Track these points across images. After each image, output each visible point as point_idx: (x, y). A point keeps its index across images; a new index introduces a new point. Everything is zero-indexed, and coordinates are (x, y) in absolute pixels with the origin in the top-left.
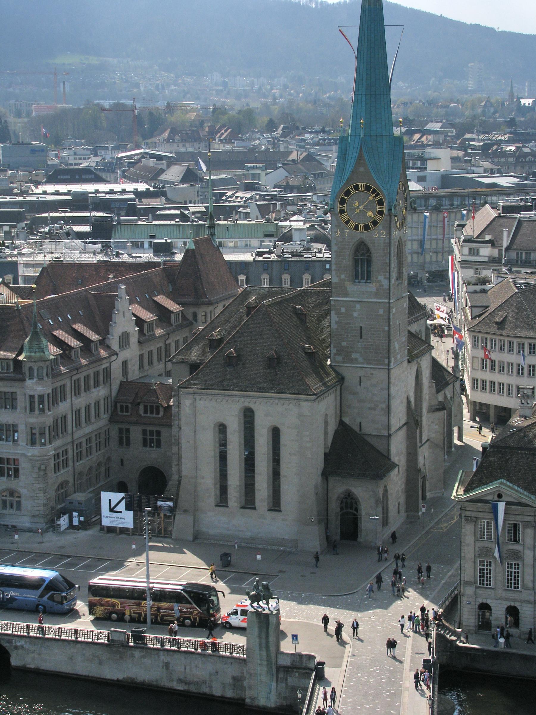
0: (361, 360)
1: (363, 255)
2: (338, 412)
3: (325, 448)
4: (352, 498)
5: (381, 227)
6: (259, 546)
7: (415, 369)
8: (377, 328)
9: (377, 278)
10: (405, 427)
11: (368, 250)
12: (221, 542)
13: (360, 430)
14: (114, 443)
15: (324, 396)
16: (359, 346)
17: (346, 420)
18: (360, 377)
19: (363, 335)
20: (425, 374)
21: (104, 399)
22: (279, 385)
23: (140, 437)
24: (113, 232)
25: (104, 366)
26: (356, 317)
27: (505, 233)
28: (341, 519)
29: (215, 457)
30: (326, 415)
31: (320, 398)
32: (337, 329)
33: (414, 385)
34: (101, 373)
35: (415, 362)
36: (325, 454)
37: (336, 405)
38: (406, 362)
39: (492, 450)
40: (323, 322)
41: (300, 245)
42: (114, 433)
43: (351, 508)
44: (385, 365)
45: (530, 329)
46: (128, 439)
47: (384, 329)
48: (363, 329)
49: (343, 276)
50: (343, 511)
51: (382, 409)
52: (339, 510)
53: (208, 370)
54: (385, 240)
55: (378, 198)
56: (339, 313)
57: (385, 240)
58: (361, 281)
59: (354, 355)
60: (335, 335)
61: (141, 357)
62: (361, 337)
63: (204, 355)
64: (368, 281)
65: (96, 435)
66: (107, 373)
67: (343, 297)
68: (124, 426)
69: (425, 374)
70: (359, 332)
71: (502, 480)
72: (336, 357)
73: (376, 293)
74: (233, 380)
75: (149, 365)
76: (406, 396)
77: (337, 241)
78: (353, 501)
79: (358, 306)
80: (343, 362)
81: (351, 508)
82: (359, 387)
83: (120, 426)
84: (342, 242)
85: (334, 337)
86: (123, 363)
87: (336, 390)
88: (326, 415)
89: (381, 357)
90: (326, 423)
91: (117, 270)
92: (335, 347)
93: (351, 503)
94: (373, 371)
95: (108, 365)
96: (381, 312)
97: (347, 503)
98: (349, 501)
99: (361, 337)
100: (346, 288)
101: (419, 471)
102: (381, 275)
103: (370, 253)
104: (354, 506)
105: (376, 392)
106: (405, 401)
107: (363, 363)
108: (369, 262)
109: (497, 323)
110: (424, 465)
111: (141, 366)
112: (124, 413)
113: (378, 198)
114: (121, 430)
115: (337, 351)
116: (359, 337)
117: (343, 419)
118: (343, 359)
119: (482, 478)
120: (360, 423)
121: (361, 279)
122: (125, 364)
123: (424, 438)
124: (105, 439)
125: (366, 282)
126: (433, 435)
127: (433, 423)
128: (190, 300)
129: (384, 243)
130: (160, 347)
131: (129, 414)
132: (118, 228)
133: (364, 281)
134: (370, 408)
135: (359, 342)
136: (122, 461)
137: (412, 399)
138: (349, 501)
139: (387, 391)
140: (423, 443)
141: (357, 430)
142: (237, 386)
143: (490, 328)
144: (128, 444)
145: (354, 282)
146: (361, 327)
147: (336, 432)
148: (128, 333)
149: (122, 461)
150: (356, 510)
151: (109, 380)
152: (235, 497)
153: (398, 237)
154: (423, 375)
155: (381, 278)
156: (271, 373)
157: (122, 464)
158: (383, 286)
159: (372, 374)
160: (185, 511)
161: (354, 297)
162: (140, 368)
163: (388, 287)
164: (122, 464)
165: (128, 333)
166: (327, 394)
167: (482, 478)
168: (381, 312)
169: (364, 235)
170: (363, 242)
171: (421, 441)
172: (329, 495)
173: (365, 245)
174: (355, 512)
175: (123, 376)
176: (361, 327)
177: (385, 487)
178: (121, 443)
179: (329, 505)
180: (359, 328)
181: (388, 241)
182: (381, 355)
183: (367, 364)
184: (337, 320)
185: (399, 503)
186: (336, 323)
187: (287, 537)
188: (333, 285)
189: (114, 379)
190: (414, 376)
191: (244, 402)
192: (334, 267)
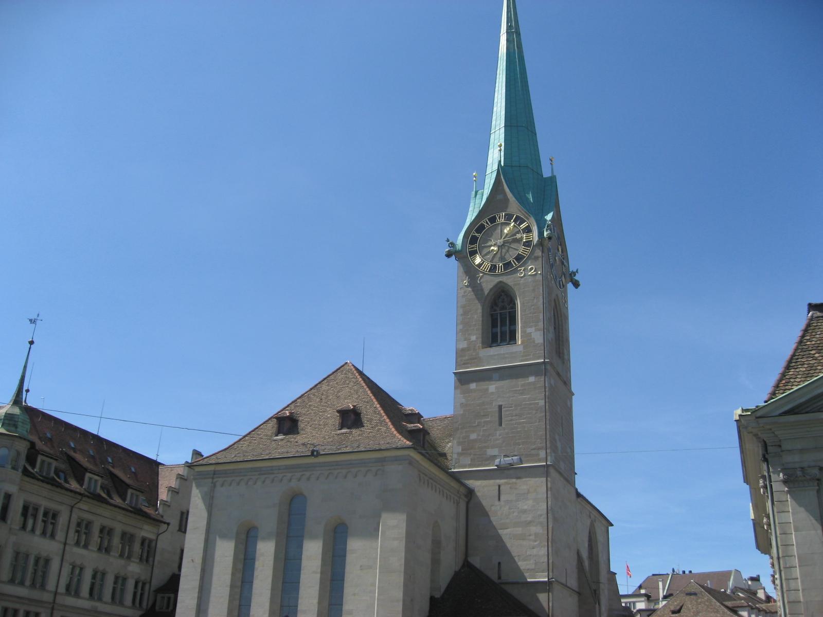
1: (503, 308)
13: (499, 578)
17: (476, 561)
18: (499, 486)
26: (492, 393)
27: (660, 584)
36: (432, 599)
44: (540, 461)
45: (715, 612)
49: (473, 338)
51: (536, 535)
58: (501, 344)
59: (491, 452)
62: (500, 424)
64: (511, 343)
70: (497, 415)
80: (470, 466)
82: (497, 503)
90: (437, 544)
102: (531, 327)
105: (526, 507)
115: (462, 450)
116: (497, 423)
117: (471, 560)
120: (499, 563)
121: (501, 343)
133: (505, 344)
137: (586, 563)
139: (546, 503)
141: (494, 577)
170: (503, 291)
176: (500, 407)
180: (497, 409)
191: (290, 480)
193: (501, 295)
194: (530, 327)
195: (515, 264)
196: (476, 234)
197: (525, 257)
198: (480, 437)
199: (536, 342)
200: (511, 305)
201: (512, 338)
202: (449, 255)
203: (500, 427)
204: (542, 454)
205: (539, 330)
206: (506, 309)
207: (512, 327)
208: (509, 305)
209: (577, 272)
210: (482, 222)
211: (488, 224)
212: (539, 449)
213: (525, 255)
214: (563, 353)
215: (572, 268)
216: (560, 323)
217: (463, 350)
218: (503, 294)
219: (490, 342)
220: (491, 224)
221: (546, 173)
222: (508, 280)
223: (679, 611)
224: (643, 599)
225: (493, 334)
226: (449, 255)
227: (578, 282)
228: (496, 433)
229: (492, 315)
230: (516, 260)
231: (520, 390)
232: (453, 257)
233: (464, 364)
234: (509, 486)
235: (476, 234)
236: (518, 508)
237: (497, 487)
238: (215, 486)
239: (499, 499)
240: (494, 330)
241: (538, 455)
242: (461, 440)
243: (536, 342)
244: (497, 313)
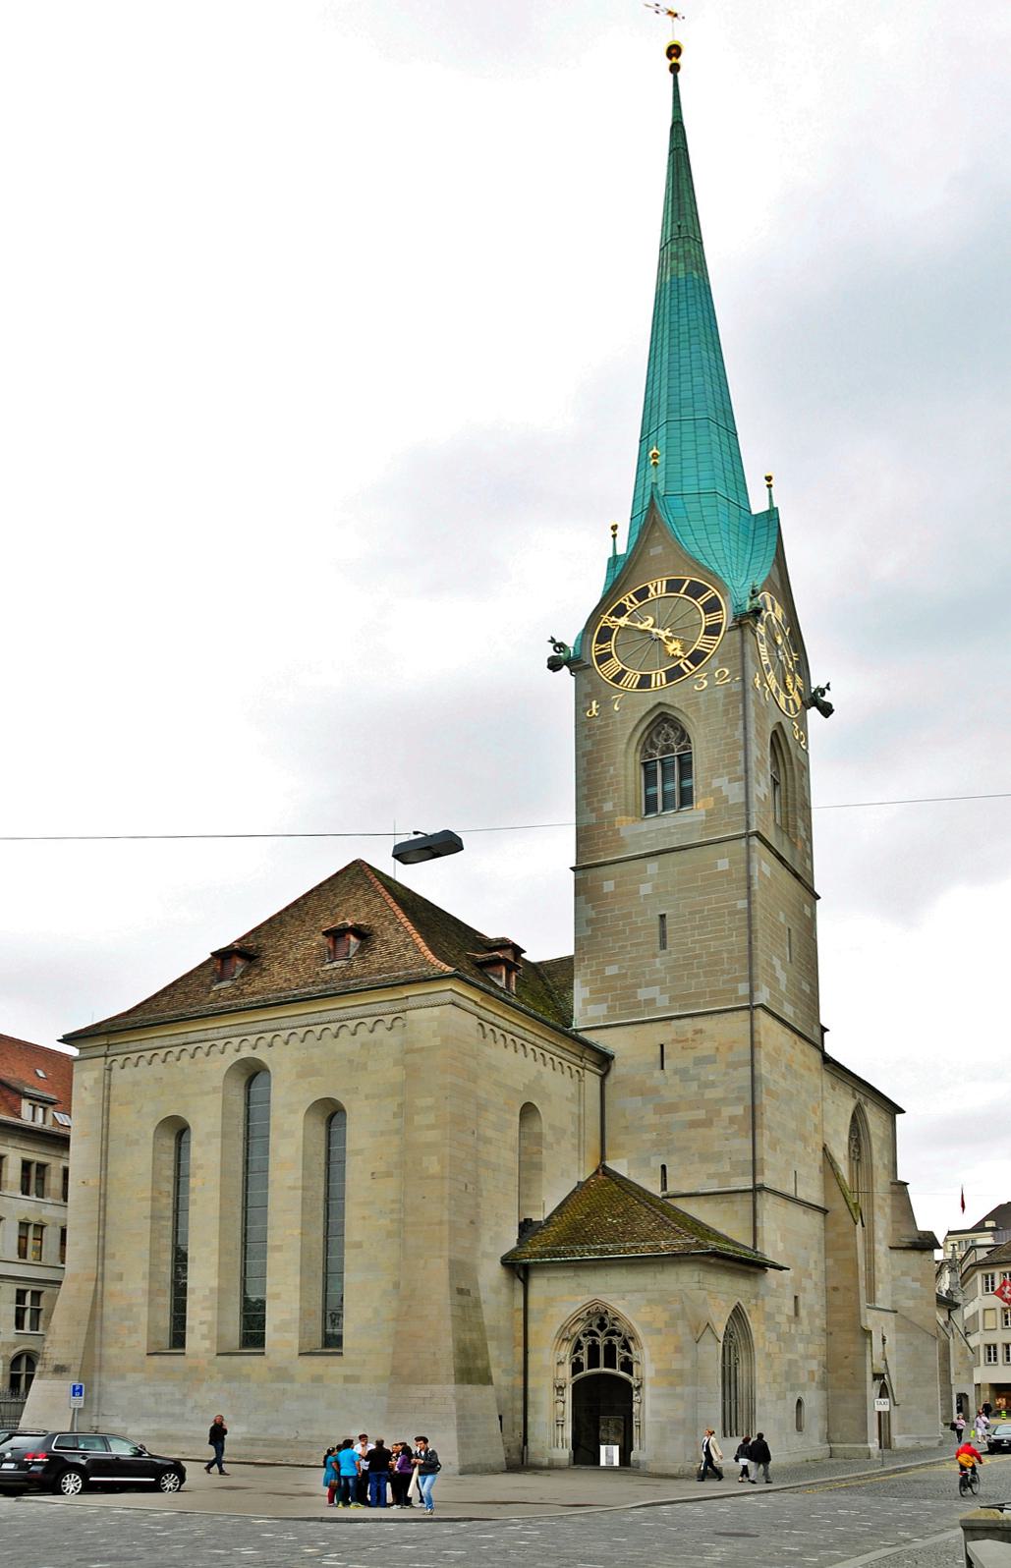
4: (612, 1333)
5: (715, 662)
8: (708, 910)
11: (684, 735)
16: (658, 966)
44: (737, 999)
70: (657, 930)
78: (616, 1340)
79: (652, 867)
81: (610, 1363)
89: (725, 982)
93: (610, 1349)
94: (700, 1023)
97: (593, 1349)
98: (602, 1341)
99: (663, 946)
104: (620, 1354)
134: (694, 1124)
138: (602, 1341)
145: (643, 819)
150: (627, 1366)
163: (742, 799)
173: (675, 724)
174: (623, 1374)
180: (657, 922)
181: (737, 688)
182: (726, 977)
193: (663, 729)
194: (718, 777)
197: (708, 654)
200: (682, 744)
201: (686, 797)
202: (554, 665)
203: (664, 951)
207: (686, 783)
208: (679, 744)
209: (829, 689)
210: (621, 601)
211: (631, 602)
212: (737, 980)
213: (708, 651)
215: (816, 682)
219: (644, 813)
220: (640, 602)
221: (758, 505)
222: (671, 695)
225: (647, 797)
226: (554, 665)
227: (831, 705)
228: (655, 962)
229: (645, 765)
230: (690, 661)
231: (698, 887)
232: (565, 669)
234: (680, 1045)
236: (699, 1080)
237: (659, 1048)
238: (110, 1070)
240: (651, 791)
241: (735, 990)
244: (656, 761)
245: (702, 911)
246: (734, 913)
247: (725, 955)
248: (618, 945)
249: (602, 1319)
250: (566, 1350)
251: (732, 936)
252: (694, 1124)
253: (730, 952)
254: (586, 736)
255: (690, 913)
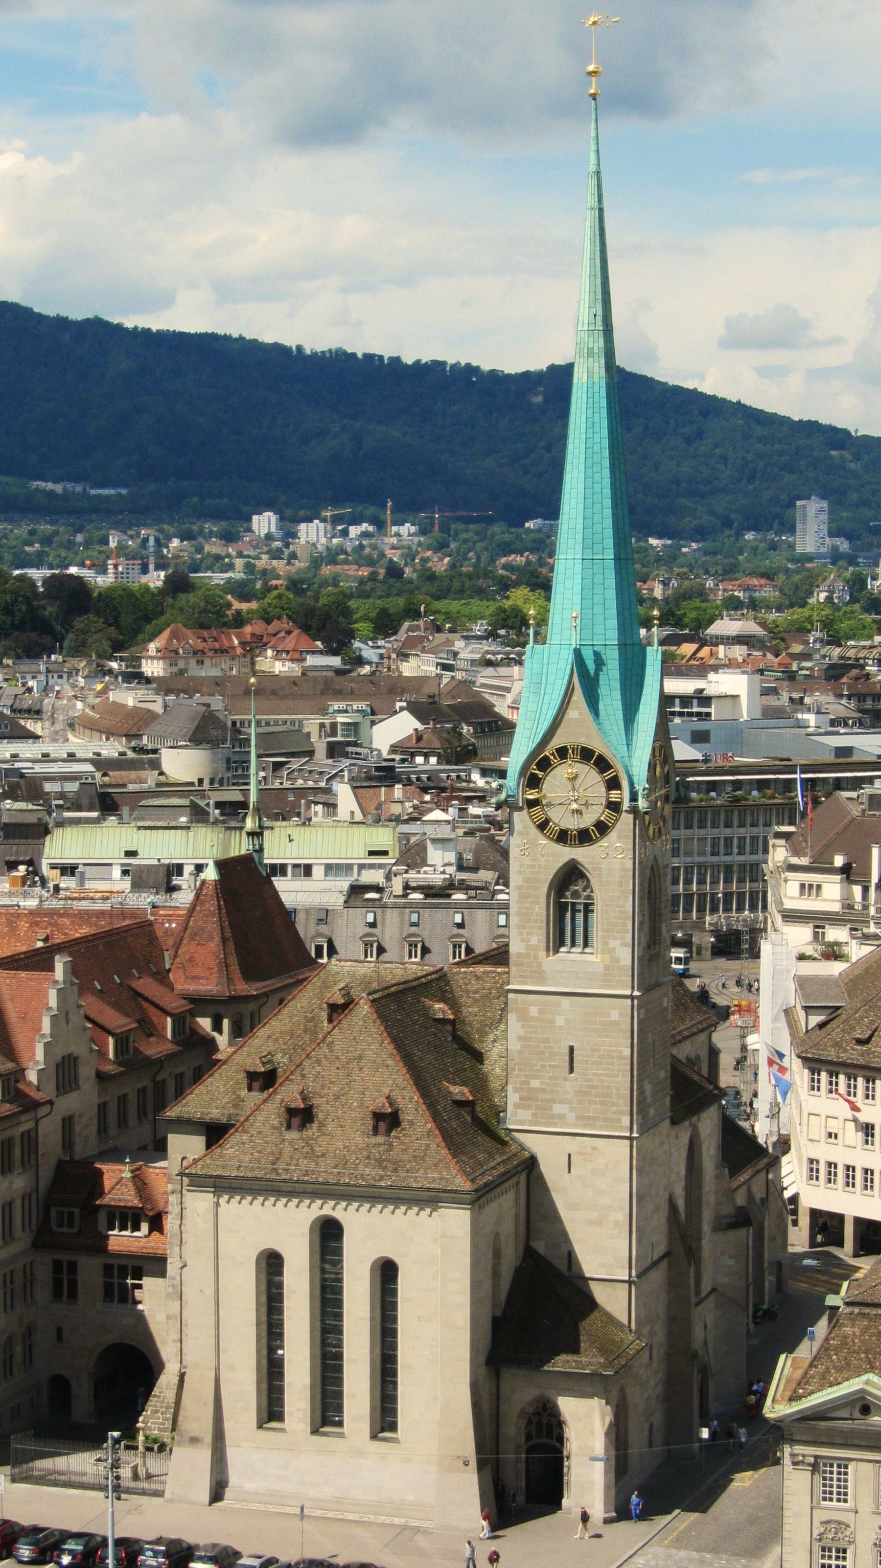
0: (571, 1117)
1: (576, 895)
2: (522, 1229)
3: (494, 1306)
6: (351, 1517)
7: (685, 1139)
9: (605, 944)
10: (664, 1264)
12: (270, 1508)
14: (43, 1294)
15: (492, 1195)
17: (540, 1246)
18: (570, 1155)
19: (575, 1065)
20: (708, 1149)
21: (23, 1198)
22: (395, 1170)
23: (99, 1280)
24: (47, 843)
25: (23, 1128)
26: (560, 1027)
28: (527, 1459)
29: (258, 1324)
30: (497, 1235)
31: (484, 1200)
32: (520, 1052)
33: (683, 1172)
34: (18, 1142)
35: (687, 1123)
37: (517, 1217)
38: (667, 1122)
39: (849, 1310)
40: (491, 1037)
41: (443, 872)
42: (44, 1273)
43: (550, 1434)
44: (622, 1129)
46: (73, 1284)
47: (621, 1051)
48: (575, 1052)
50: (531, 1443)
51: (616, 1223)
52: (523, 1437)
53: (245, 1137)
54: (623, 864)
55: (609, 775)
56: (524, 1018)
57: (623, 864)
58: (573, 950)
59: (558, 1109)
60: (516, 1064)
61: (102, 1108)
62: (571, 1070)
63: (236, 1106)
64: (587, 950)
65: (5, 1275)
66: (30, 1141)
67: (532, 984)
68: (65, 1257)
69: (708, 1149)
70: (567, 1058)
71: (870, 1376)
72: (519, 1111)
73: (605, 975)
74: (298, 1160)
75: (119, 1126)
76: (667, 1197)
77: (521, 865)
78: (554, 1421)
80: (531, 1123)
82: (566, 1175)
83: (57, 1256)
84: (533, 866)
85: (514, 1069)
86: (63, 1120)
87: (518, 1183)
88: (497, 1235)
89: (614, 1112)
90: (497, 1253)
91: (56, 924)
92: (516, 1090)
93: (549, 1425)
95: (29, 1126)
96: (615, 1016)
97: (539, 1423)
99: (571, 1070)
100: (540, 965)
101: (695, 1355)
103: (592, 891)
106: (665, 1206)
107: (574, 1126)
108: (588, 909)
109: (859, 1042)
110: (705, 1343)
111: (102, 1129)
112: (65, 1229)
113: (609, 775)
114: (57, 1266)
115: (521, 1099)
116: (567, 1069)
118: (534, 1115)
119: (827, 1370)
122: (68, 1122)
123: (706, 1285)
124: (25, 1284)
125: (582, 953)
126: (725, 1280)
127: (723, 1253)
128: (209, 988)
129: (623, 870)
130: (144, 1089)
131: (75, 1230)
132: (58, 833)
133: (579, 950)
134: (591, 1222)
135: (566, 1079)
136: (59, 1330)
137: (681, 1203)
138: (545, 1420)
140: (703, 1295)
142: (307, 1174)
143: (845, 1051)
144: (73, 1294)
146: (572, 1049)
147: (518, 1272)
148: (76, 1059)
149: (59, 1330)
151: (33, 1157)
152: (298, 1410)
153: (652, 857)
154: (704, 1149)
155: (614, 943)
156: (380, 1144)
157: (60, 1338)
158: (618, 961)
159: (594, 1148)
160: (194, 1440)
161: (556, 985)
162: (99, 1133)
164: (60, 1338)
165: (76, 1059)
166: (498, 1190)
167: (827, 1370)
168: (615, 1016)
169: (580, 854)
171: (698, 1293)
172: (503, 1408)
173: (582, 875)
175: (64, 1148)
176: (572, 1049)
177: (622, 1390)
178: (57, 1294)
179: (502, 1430)
180: (567, 1051)
182: (615, 1109)
183: (585, 1126)
184: (522, 1032)
185: (651, 1425)
186: (520, 1038)
187: (411, 1498)
188: (512, 959)
189: (43, 1155)
190: (684, 1153)
192: (513, 920)
193: (574, 873)
195: (595, 835)
196: (537, 772)
198: (544, 1086)
199: (622, 963)
204: (626, 1120)
205: (626, 945)
206: (579, 897)
211: (555, 758)
212: (621, 1113)
214: (660, 934)
216: (658, 887)
217: (519, 955)
218: (576, 872)
223: (867, 1041)
224: (838, 878)
233: (520, 976)
235: (537, 772)
239: (569, 1172)
241: (619, 1121)
242: (518, 1085)
243: (622, 963)
245: (598, 1050)
246: (622, 1058)
247: (614, 1091)
248: (540, 1063)
249: (545, 1404)
250: (523, 1423)
251: (618, 1076)
252: (591, 1222)
253: (617, 1089)
254: (519, 871)
255: (592, 1050)
